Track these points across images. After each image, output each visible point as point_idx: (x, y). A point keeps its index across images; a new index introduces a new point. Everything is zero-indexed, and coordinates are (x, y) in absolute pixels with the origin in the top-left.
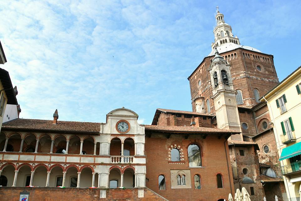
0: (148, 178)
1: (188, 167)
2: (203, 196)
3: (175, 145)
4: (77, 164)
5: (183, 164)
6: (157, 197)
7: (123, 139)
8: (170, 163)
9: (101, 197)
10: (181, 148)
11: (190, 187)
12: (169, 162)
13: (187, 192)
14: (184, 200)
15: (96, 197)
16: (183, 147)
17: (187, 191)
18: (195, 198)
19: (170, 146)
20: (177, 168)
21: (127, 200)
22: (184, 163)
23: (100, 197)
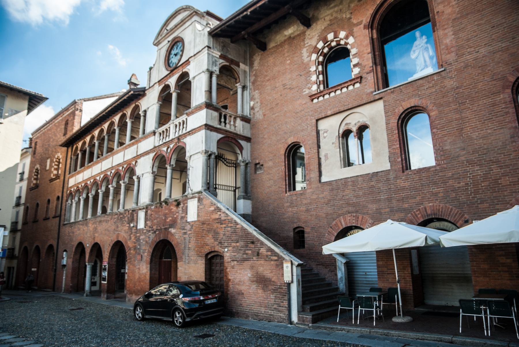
0: (261, 164)
1: (372, 92)
2: (441, 195)
3: (330, 36)
4: (120, 166)
5: (357, 85)
6: (223, 215)
7: (172, 81)
8: (315, 101)
9: (140, 226)
10: (347, 37)
11: (387, 166)
12: (312, 97)
13: (373, 186)
14: (360, 218)
15: (133, 227)
16: (355, 29)
17: (373, 183)
18: (406, 206)
19: (316, 47)
20: (336, 110)
21: (170, 229)
22: (360, 83)
23: (138, 228)
